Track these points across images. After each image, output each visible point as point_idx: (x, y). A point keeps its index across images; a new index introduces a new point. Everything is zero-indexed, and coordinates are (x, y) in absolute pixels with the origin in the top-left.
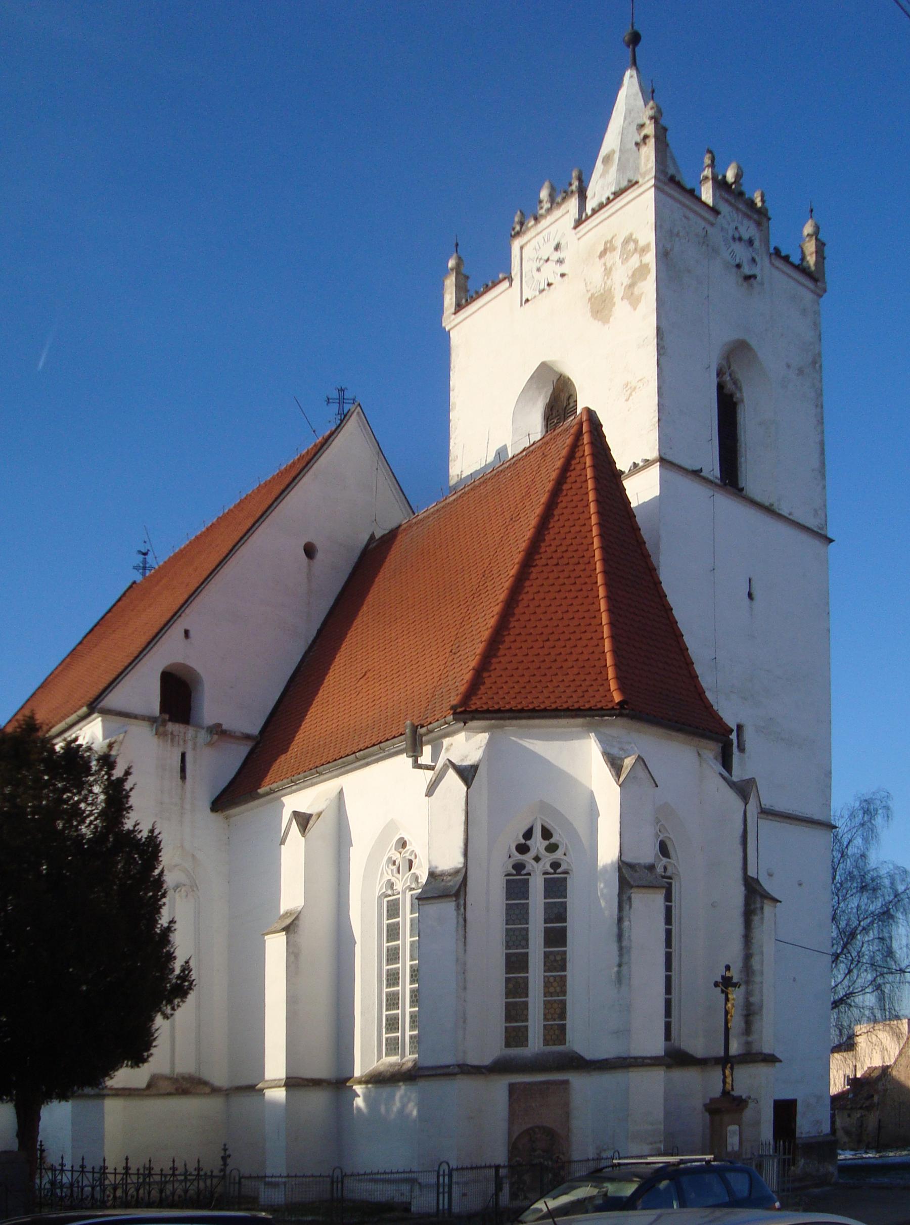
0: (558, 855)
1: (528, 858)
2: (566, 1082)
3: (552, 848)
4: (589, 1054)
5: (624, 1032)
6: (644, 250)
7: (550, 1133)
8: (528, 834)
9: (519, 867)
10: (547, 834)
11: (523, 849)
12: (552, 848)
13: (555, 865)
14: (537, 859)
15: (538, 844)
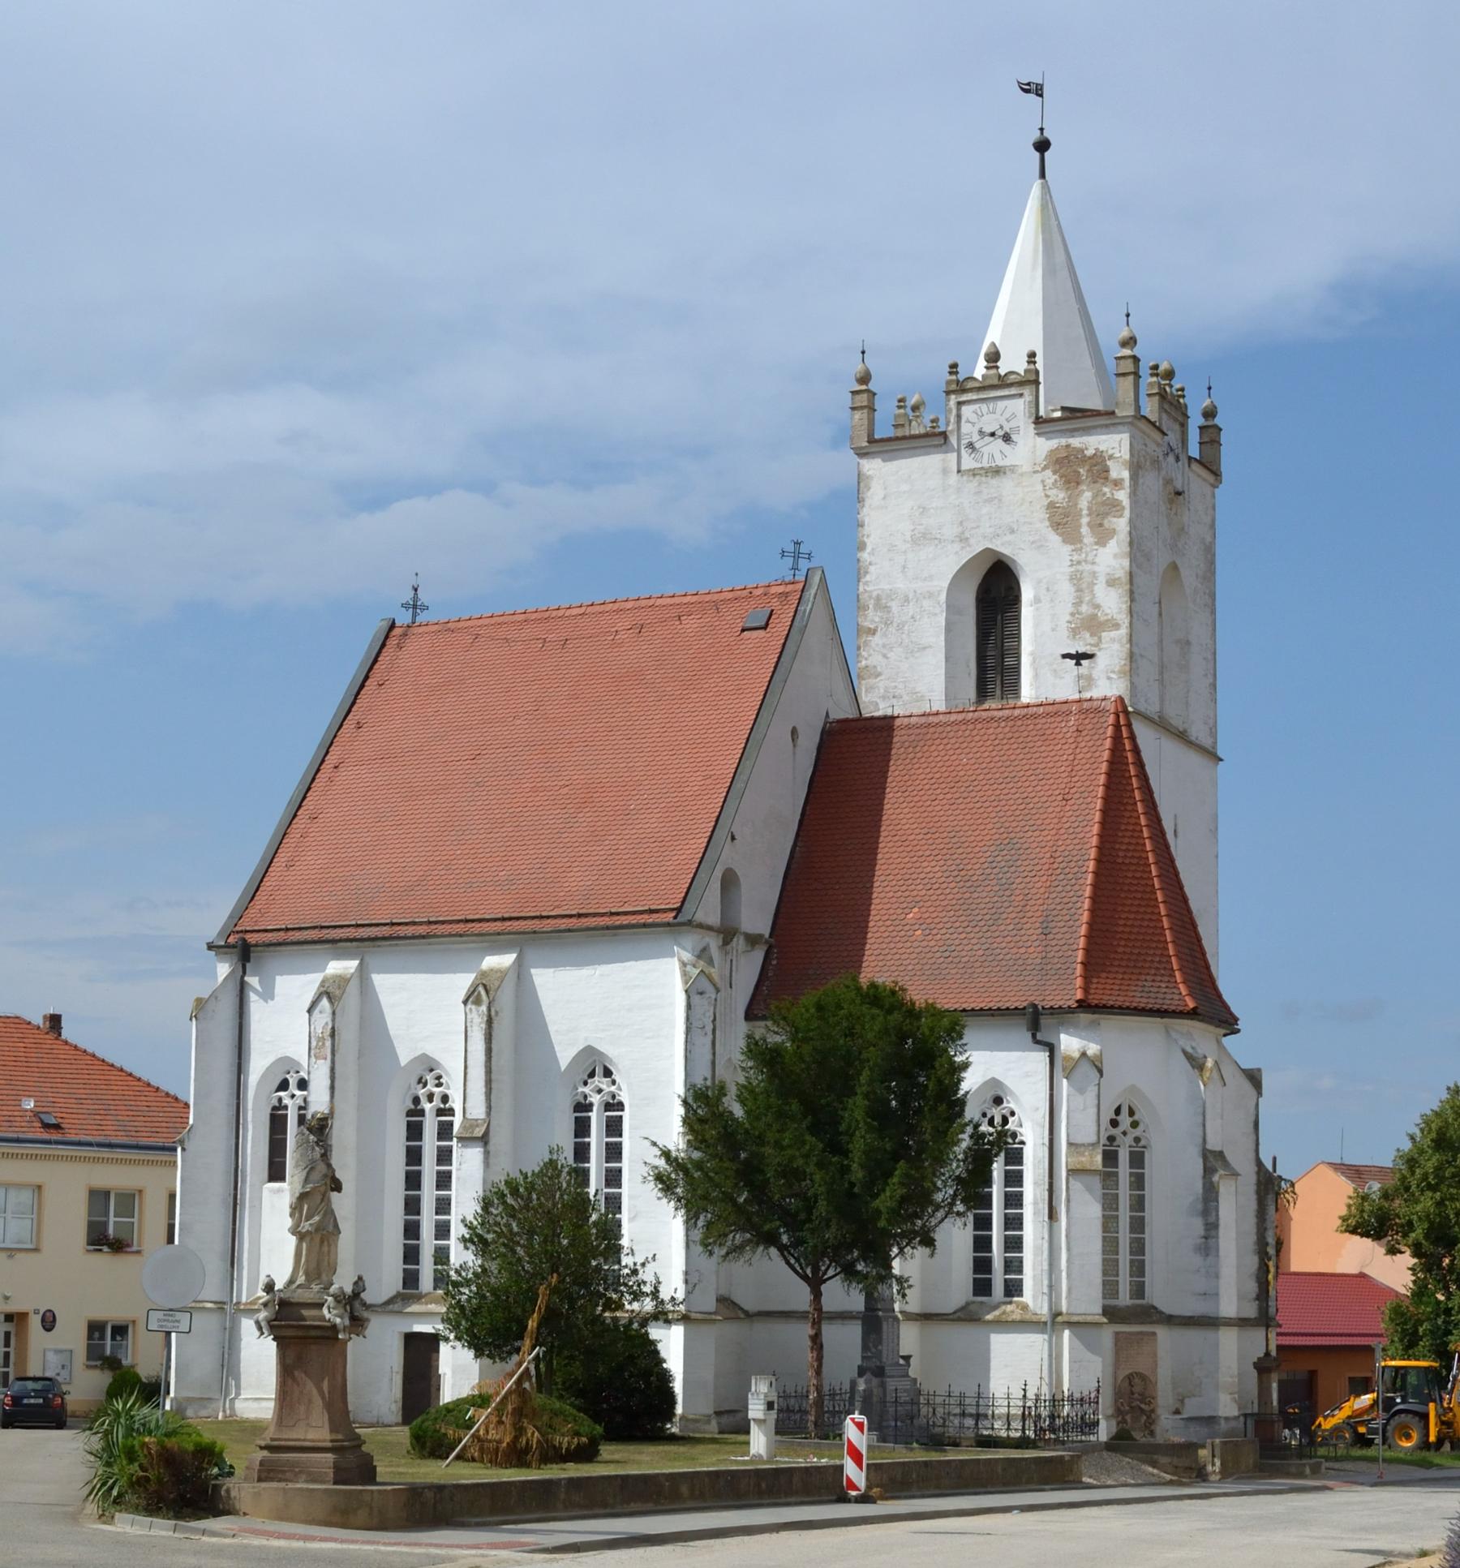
0: (1141, 1128)
1: (1116, 1132)
2: (1154, 1334)
3: (1135, 1125)
4: (1167, 1308)
5: (1213, 1295)
6: (1117, 483)
7: (1143, 1378)
8: (1118, 1111)
9: (1111, 1139)
10: (1131, 1113)
11: (1114, 1123)
12: (1135, 1125)
13: (1137, 1140)
14: (1124, 1133)
15: (1125, 1120)
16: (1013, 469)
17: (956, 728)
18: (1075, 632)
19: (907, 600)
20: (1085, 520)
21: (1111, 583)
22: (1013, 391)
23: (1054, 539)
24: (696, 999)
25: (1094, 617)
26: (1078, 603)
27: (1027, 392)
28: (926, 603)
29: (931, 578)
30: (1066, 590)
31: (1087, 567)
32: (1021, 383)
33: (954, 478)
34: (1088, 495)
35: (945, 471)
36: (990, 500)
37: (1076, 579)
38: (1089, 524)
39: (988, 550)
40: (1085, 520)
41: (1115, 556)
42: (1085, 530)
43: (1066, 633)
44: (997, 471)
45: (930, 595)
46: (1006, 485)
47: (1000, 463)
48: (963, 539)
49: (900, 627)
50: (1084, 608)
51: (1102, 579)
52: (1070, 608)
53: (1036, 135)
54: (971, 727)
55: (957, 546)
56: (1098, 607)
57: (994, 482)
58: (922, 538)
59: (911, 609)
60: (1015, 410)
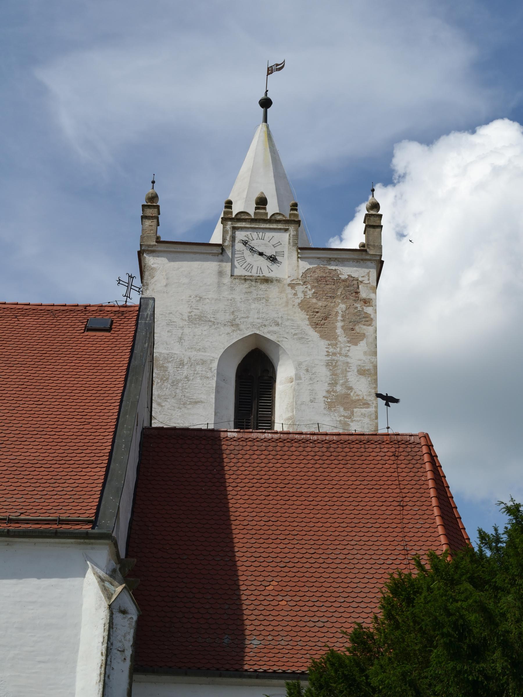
16: (278, 281)
17: (274, 444)
18: (330, 406)
19: (182, 364)
20: (339, 324)
21: (362, 372)
22: (280, 226)
23: (313, 334)
24: (118, 617)
25: (347, 396)
26: (333, 383)
27: (292, 228)
28: (199, 368)
29: (204, 349)
30: (323, 372)
31: (338, 358)
32: (287, 222)
33: (227, 280)
34: (343, 306)
35: (221, 273)
36: (258, 299)
37: (331, 365)
38: (343, 327)
39: (256, 336)
40: (339, 324)
41: (365, 353)
42: (339, 331)
43: (323, 405)
44: (267, 280)
45: (203, 362)
46: (273, 291)
47: (266, 274)
48: (234, 324)
49: (175, 383)
50: (339, 388)
51: (354, 369)
52: (326, 387)
53: (263, 96)
54: (289, 444)
55: (229, 329)
56: (351, 388)
57: (263, 287)
58: (197, 319)
59: (185, 371)
60: (281, 240)
